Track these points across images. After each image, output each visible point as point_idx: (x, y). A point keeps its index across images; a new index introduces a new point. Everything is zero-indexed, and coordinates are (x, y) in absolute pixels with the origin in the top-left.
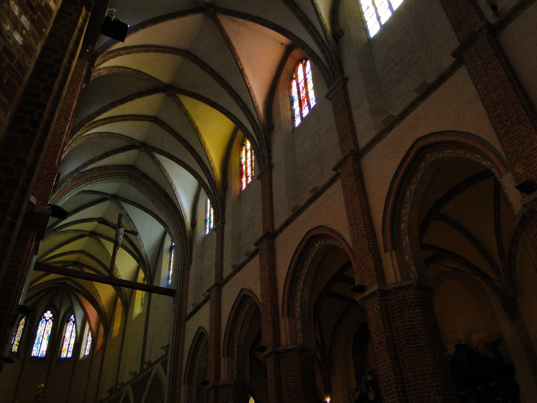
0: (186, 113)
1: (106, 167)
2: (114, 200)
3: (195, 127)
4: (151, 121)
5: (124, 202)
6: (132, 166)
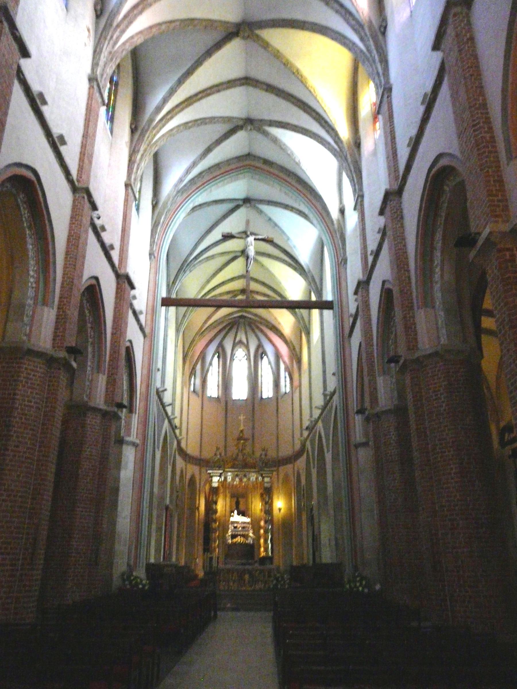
0: (277, 55)
1: (217, 166)
2: (248, 205)
3: (294, 71)
4: (242, 85)
5: (260, 204)
6: (249, 155)
